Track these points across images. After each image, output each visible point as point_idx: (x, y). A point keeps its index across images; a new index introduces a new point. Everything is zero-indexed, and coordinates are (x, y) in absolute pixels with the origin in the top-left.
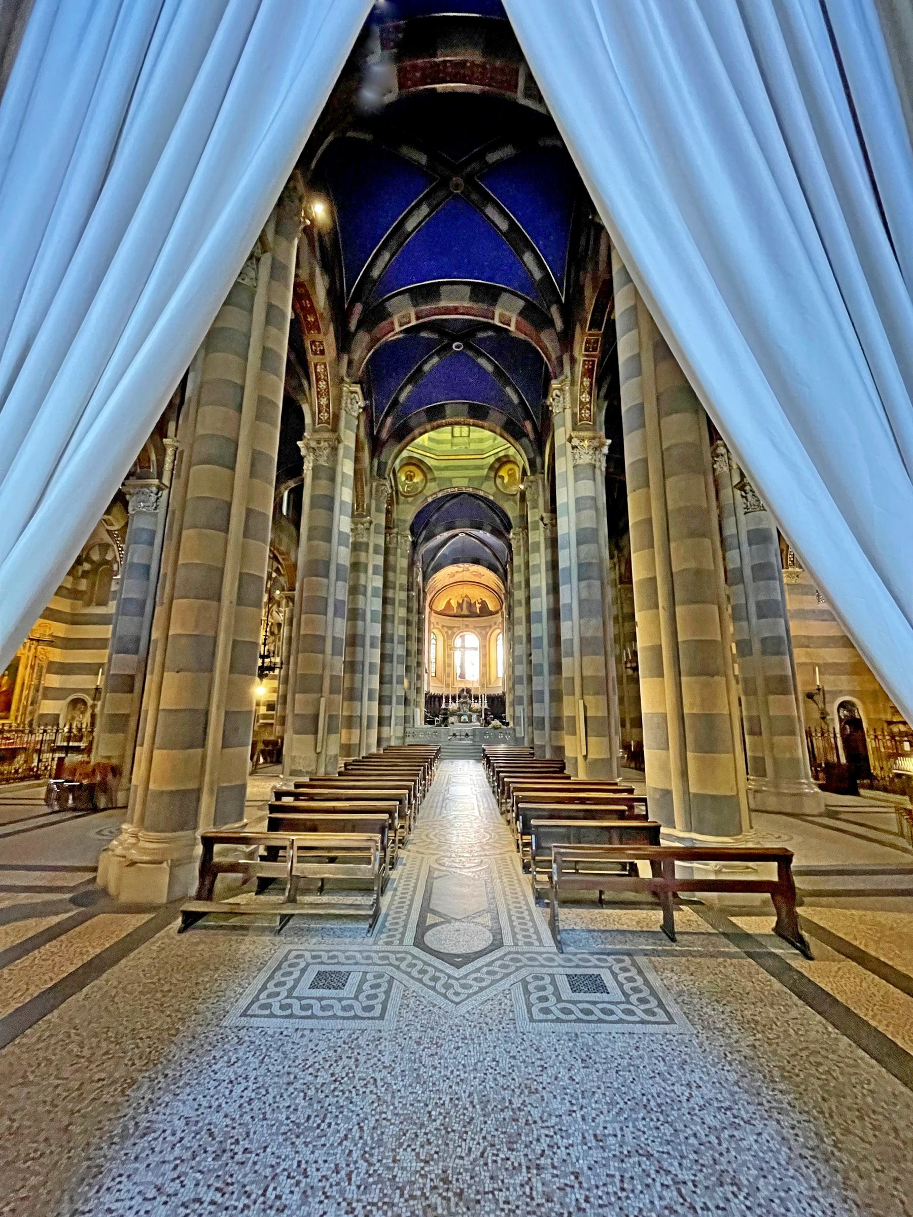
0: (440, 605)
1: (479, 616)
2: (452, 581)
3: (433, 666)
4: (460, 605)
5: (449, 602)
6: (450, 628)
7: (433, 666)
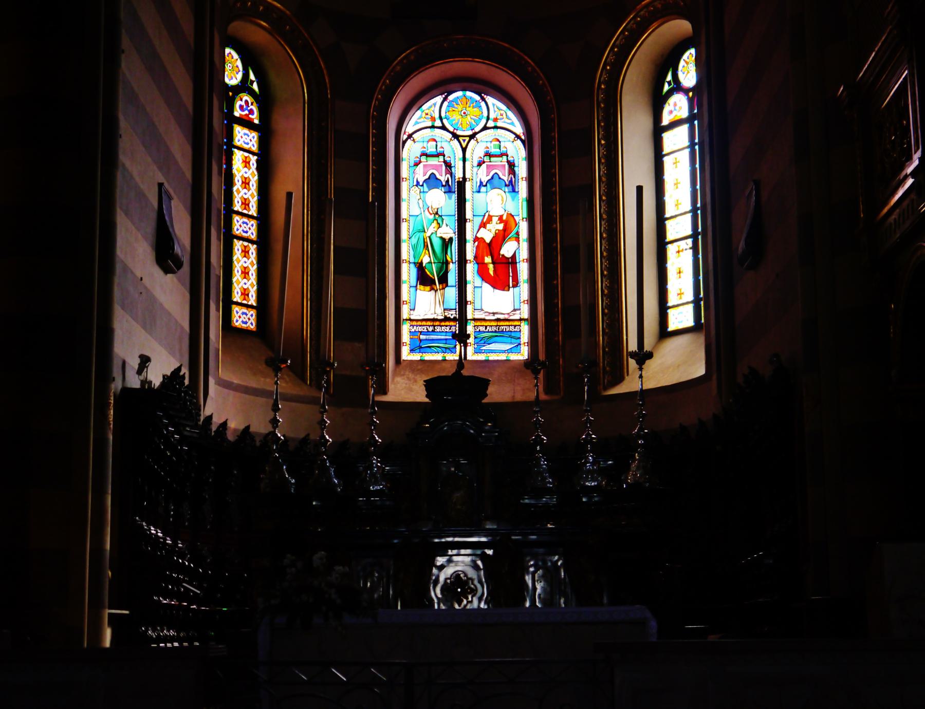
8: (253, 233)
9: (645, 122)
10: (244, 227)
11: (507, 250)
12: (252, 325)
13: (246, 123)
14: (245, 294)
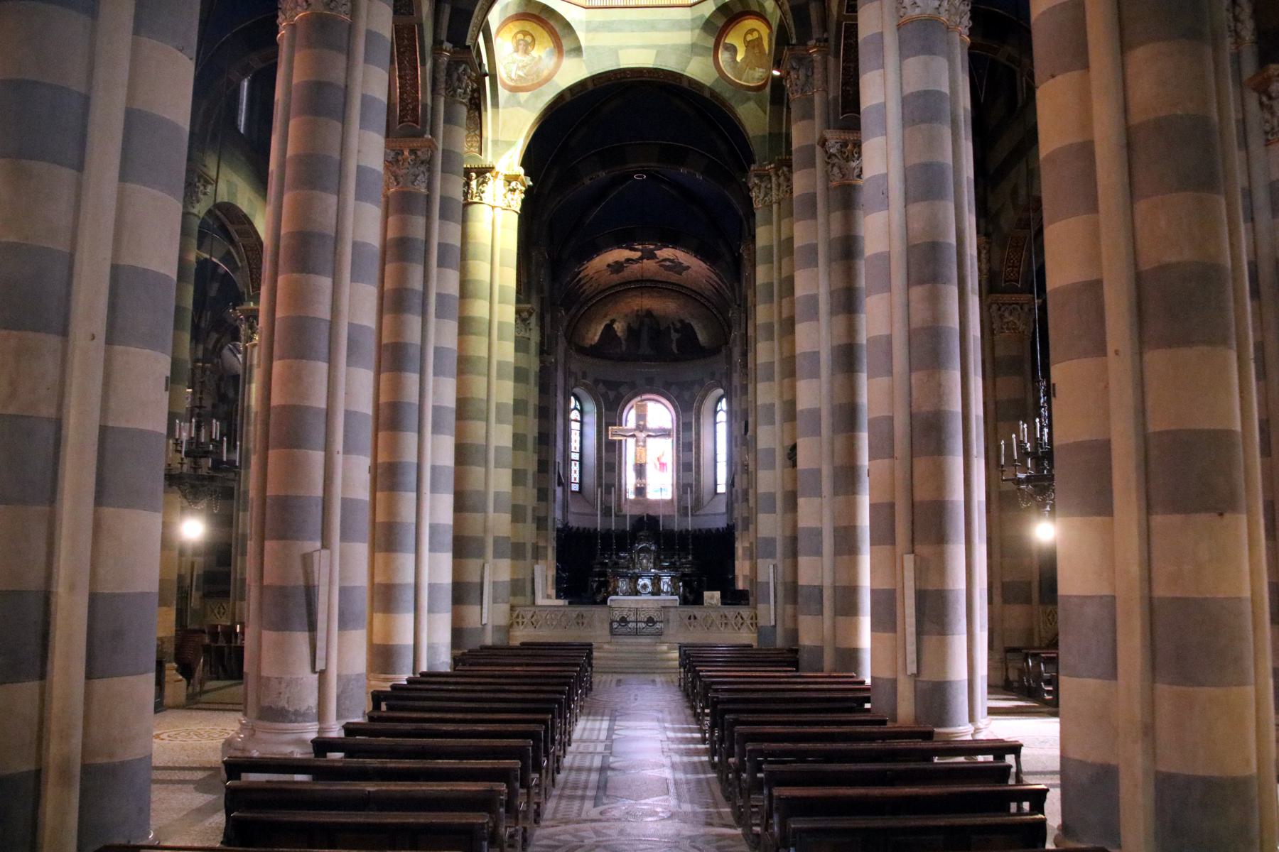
0: (594, 334)
1: (676, 359)
2: (616, 278)
3: (575, 468)
4: (632, 332)
5: (609, 328)
7: (575, 468)
8: (578, 458)
9: (712, 420)
10: (575, 456)
11: (663, 460)
12: (577, 489)
13: (576, 421)
14: (575, 479)
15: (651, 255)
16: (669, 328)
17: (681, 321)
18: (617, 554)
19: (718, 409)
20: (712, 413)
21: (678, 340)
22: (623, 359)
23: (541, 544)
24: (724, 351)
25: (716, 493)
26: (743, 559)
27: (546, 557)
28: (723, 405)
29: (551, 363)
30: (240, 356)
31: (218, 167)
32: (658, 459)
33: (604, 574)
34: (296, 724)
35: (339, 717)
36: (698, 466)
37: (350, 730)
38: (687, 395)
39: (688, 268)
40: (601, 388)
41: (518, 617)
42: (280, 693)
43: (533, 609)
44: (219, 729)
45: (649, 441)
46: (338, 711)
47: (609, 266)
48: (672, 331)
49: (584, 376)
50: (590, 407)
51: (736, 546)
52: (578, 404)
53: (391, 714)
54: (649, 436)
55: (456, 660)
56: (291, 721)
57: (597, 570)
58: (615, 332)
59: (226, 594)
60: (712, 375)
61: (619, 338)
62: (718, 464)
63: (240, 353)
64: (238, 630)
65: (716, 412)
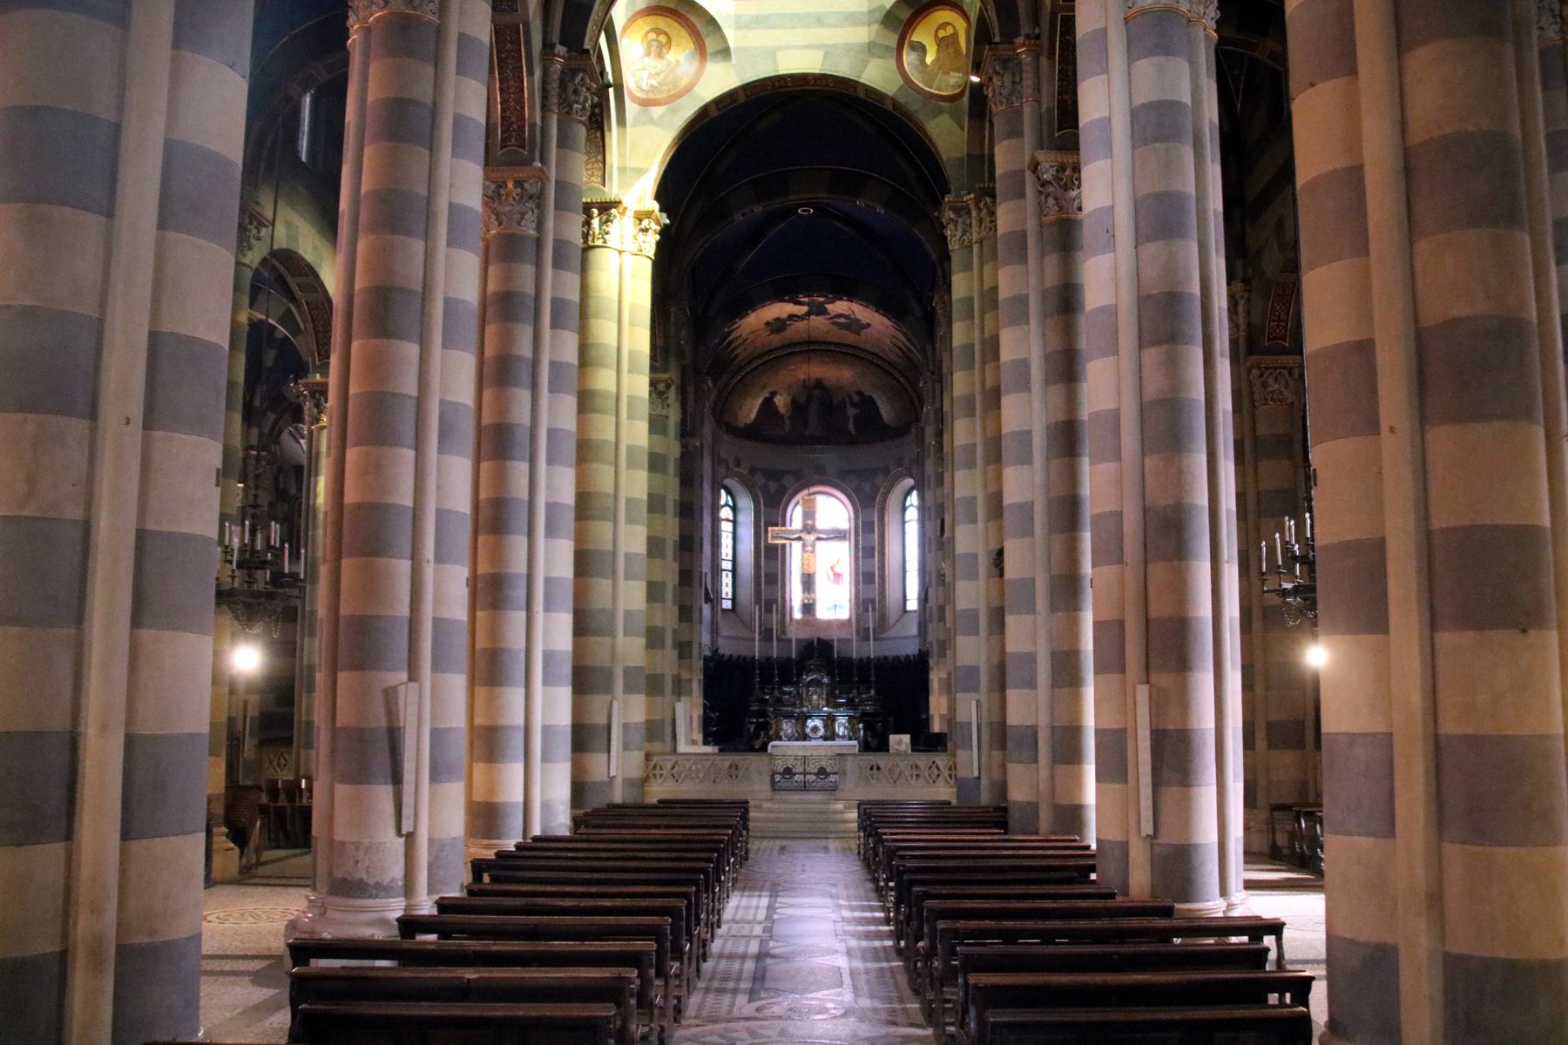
0: (750, 410)
1: (853, 441)
2: (776, 339)
3: (727, 579)
4: (797, 407)
5: (768, 402)
6: (773, 475)
7: (727, 579)
8: (730, 568)
9: (898, 517)
10: (727, 565)
11: (838, 570)
13: (728, 520)
14: (727, 594)
15: (821, 311)
16: (844, 402)
17: (860, 393)
18: (780, 689)
19: (907, 504)
20: (899, 508)
21: (855, 417)
22: (787, 441)
23: (685, 675)
24: (913, 430)
25: (905, 611)
26: (940, 694)
27: (690, 693)
28: (913, 499)
29: (695, 447)
30: (302, 441)
31: (276, 203)
32: (832, 568)
33: (763, 714)
34: (378, 900)
35: (431, 891)
36: (882, 577)
37: (444, 906)
38: (867, 487)
39: (868, 325)
40: (760, 479)
41: (654, 768)
42: (357, 862)
43: (674, 758)
44: (280, 908)
45: (819, 544)
46: (429, 884)
47: (767, 324)
48: (848, 403)
49: (738, 464)
50: (746, 503)
51: (931, 676)
52: (729, 498)
53: (497, 887)
54: (819, 539)
55: (577, 822)
56: (371, 897)
57: (755, 708)
58: (775, 407)
59: (288, 741)
60: (900, 462)
61: (782, 416)
62: (908, 574)
63: (303, 437)
64: (303, 786)
65: (904, 509)
